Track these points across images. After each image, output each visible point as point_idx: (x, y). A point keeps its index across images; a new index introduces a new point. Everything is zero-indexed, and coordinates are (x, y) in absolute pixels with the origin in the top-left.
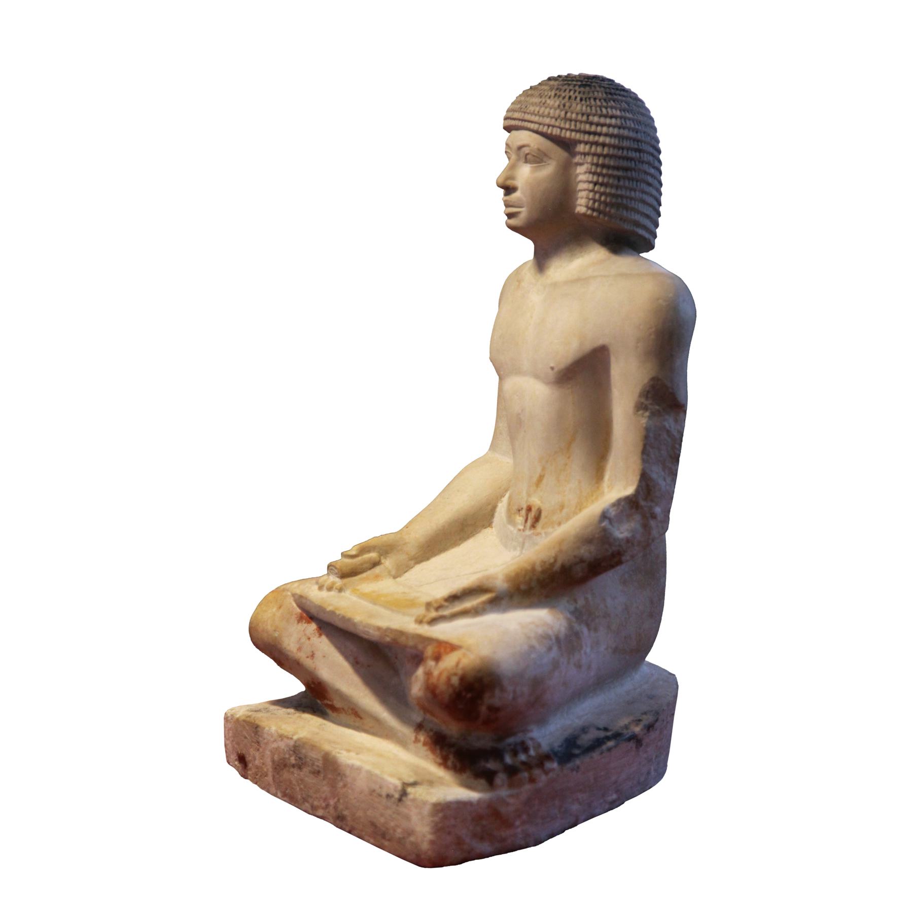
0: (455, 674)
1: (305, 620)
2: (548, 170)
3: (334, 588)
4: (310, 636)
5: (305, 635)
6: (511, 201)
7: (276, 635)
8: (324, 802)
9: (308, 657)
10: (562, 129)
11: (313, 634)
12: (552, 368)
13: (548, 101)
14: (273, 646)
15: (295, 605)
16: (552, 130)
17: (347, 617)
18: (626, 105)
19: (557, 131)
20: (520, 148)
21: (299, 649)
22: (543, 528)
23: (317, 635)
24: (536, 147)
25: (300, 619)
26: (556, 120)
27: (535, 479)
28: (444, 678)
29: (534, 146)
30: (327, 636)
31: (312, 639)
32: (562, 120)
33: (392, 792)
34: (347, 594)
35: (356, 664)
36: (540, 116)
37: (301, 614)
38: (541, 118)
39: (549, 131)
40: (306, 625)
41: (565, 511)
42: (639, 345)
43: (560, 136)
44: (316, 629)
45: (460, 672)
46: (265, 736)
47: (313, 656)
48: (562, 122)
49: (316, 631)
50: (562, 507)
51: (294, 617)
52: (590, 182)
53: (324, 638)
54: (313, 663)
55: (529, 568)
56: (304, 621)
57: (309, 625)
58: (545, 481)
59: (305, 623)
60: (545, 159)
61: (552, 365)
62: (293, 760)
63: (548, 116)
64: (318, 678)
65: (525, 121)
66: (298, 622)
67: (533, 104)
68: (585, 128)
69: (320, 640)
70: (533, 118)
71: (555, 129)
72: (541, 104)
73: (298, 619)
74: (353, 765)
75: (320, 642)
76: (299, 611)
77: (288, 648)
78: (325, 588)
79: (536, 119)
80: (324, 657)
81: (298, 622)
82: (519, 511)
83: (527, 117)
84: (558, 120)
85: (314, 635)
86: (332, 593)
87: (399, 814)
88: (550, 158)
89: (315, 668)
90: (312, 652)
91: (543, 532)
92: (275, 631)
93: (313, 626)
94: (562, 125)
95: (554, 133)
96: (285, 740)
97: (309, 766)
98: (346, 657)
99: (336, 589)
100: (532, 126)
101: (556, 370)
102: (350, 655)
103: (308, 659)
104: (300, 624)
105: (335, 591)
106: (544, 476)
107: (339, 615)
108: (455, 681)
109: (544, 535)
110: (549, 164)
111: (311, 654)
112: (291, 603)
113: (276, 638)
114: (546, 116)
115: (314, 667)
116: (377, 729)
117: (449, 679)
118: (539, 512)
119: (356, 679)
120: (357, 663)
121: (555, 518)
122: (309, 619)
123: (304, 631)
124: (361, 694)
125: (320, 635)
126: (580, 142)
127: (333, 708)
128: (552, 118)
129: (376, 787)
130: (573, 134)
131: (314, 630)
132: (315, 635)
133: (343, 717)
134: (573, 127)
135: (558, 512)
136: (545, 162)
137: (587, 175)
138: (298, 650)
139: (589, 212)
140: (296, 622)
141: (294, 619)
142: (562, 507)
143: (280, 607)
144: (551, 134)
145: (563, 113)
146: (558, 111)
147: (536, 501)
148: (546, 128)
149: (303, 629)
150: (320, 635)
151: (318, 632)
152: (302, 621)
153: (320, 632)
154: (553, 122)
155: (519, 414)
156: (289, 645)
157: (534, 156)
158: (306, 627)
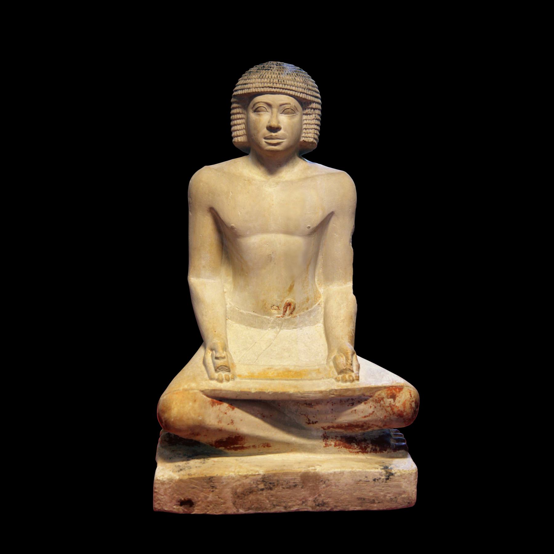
0: (413, 401)
1: (217, 403)
2: (296, 119)
3: (230, 378)
4: (226, 412)
5: (222, 412)
6: (279, 136)
7: (200, 418)
8: (296, 501)
9: (229, 424)
10: (307, 94)
11: (227, 409)
12: (309, 227)
13: (296, 78)
14: (199, 426)
15: (205, 397)
16: (302, 95)
17: (279, 392)
18: (245, 78)
19: (305, 96)
20: (281, 105)
21: (220, 421)
22: (296, 313)
23: (231, 409)
24: (294, 105)
25: (213, 404)
26: (304, 89)
27: (288, 288)
28: (408, 405)
29: (293, 104)
30: (238, 408)
31: (227, 413)
32: (307, 90)
33: (378, 476)
34: (238, 379)
35: (263, 417)
36: (296, 87)
37: (212, 400)
38: (297, 88)
39: (301, 96)
40: (219, 406)
41: (310, 301)
42: (350, 209)
43: (299, 97)
44: (229, 406)
45: (414, 399)
46: (224, 481)
47: (232, 422)
48: (307, 90)
49: (229, 407)
50: (308, 300)
51: (208, 404)
52: (315, 124)
53: (236, 410)
54: (234, 426)
55: (351, 335)
56: (217, 404)
57: (222, 405)
58: (295, 288)
59: (218, 405)
60: (296, 111)
61: (309, 226)
62: (261, 486)
63: (300, 87)
64: (238, 434)
65: (286, 89)
66: (213, 406)
67: (289, 80)
68: (297, 94)
69: (234, 411)
70: (291, 88)
71: (304, 94)
72: (261, 77)
73: (211, 404)
74: (335, 473)
75: (235, 413)
76: (209, 399)
77: (210, 423)
78: (224, 380)
79: (294, 88)
80: (242, 420)
81: (213, 406)
82: (272, 307)
83: (286, 87)
84: (305, 90)
85: (228, 410)
86: (231, 382)
87: (389, 486)
88: (298, 111)
89: (237, 429)
90: (232, 420)
91: (297, 315)
92: (199, 416)
93: (225, 405)
94: (308, 93)
95: (303, 97)
96: (250, 477)
97: (299, 485)
98: (256, 416)
99: (232, 378)
100: (291, 92)
101: (311, 228)
102: (258, 414)
103: (229, 425)
104: (214, 407)
105: (231, 380)
106: (293, 286)
107: (269, 392)
108: (413, 405)
109: (298, 317)
110: (297, 115)
111: (231, 421)
112: (202, 396)
113: (201, 420)
114: (299, 87)
115: (236, 429)
116: (288, 447)
117: (411, 405)
118: (295, 304)
119: (267, 426)
120: (264, 417)
121: (304, 306)
122: (220, 402)
123: (219, 410)
124: (273, 433)
125: (233, 409)
126: (314, 102)
127: (243, 448)
128: (302, 88)
129: (358, 479)
130: (312, 97)
131: (227, 407)
132: (229, 410)
133: (246, 451)
134: (312, 94)
135: (306, 302)
136: (296, 113)
137: (314, 120)
138: (218, 422)
139: (315, 141)
140: (211, 406)
141: (209, 405)
142: (308, 300)
143: (195, 401)
144: (297, 96)
145: (306, 85)
146: (303, 84)
147: (288, 299)
148: (299, 93)
149: (218, 408)
150: (233, 409)
151: (231, 407)
152: (215, 405)
153: (233, 407)
154: (303, 91)
155: (270, 255)
156: (210, 421)
157: (292, 110)
158: (220, 407)
